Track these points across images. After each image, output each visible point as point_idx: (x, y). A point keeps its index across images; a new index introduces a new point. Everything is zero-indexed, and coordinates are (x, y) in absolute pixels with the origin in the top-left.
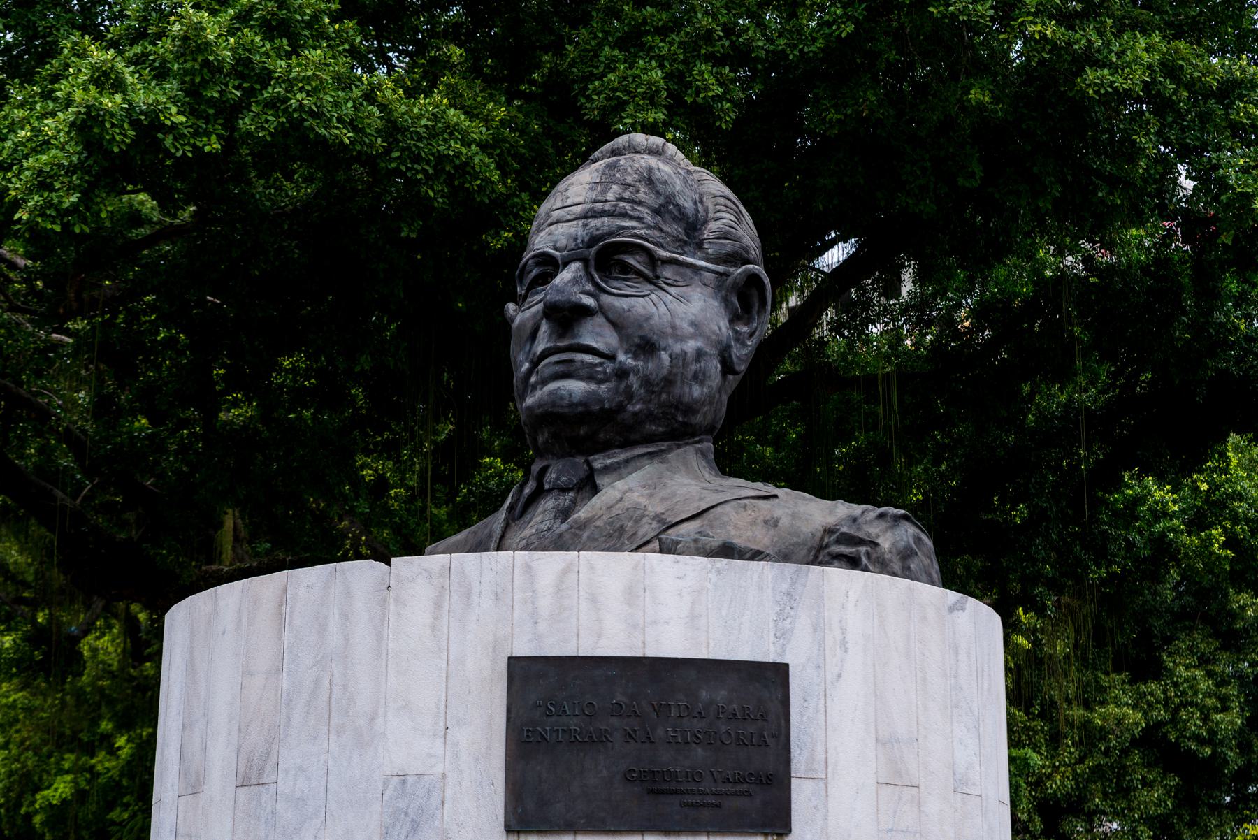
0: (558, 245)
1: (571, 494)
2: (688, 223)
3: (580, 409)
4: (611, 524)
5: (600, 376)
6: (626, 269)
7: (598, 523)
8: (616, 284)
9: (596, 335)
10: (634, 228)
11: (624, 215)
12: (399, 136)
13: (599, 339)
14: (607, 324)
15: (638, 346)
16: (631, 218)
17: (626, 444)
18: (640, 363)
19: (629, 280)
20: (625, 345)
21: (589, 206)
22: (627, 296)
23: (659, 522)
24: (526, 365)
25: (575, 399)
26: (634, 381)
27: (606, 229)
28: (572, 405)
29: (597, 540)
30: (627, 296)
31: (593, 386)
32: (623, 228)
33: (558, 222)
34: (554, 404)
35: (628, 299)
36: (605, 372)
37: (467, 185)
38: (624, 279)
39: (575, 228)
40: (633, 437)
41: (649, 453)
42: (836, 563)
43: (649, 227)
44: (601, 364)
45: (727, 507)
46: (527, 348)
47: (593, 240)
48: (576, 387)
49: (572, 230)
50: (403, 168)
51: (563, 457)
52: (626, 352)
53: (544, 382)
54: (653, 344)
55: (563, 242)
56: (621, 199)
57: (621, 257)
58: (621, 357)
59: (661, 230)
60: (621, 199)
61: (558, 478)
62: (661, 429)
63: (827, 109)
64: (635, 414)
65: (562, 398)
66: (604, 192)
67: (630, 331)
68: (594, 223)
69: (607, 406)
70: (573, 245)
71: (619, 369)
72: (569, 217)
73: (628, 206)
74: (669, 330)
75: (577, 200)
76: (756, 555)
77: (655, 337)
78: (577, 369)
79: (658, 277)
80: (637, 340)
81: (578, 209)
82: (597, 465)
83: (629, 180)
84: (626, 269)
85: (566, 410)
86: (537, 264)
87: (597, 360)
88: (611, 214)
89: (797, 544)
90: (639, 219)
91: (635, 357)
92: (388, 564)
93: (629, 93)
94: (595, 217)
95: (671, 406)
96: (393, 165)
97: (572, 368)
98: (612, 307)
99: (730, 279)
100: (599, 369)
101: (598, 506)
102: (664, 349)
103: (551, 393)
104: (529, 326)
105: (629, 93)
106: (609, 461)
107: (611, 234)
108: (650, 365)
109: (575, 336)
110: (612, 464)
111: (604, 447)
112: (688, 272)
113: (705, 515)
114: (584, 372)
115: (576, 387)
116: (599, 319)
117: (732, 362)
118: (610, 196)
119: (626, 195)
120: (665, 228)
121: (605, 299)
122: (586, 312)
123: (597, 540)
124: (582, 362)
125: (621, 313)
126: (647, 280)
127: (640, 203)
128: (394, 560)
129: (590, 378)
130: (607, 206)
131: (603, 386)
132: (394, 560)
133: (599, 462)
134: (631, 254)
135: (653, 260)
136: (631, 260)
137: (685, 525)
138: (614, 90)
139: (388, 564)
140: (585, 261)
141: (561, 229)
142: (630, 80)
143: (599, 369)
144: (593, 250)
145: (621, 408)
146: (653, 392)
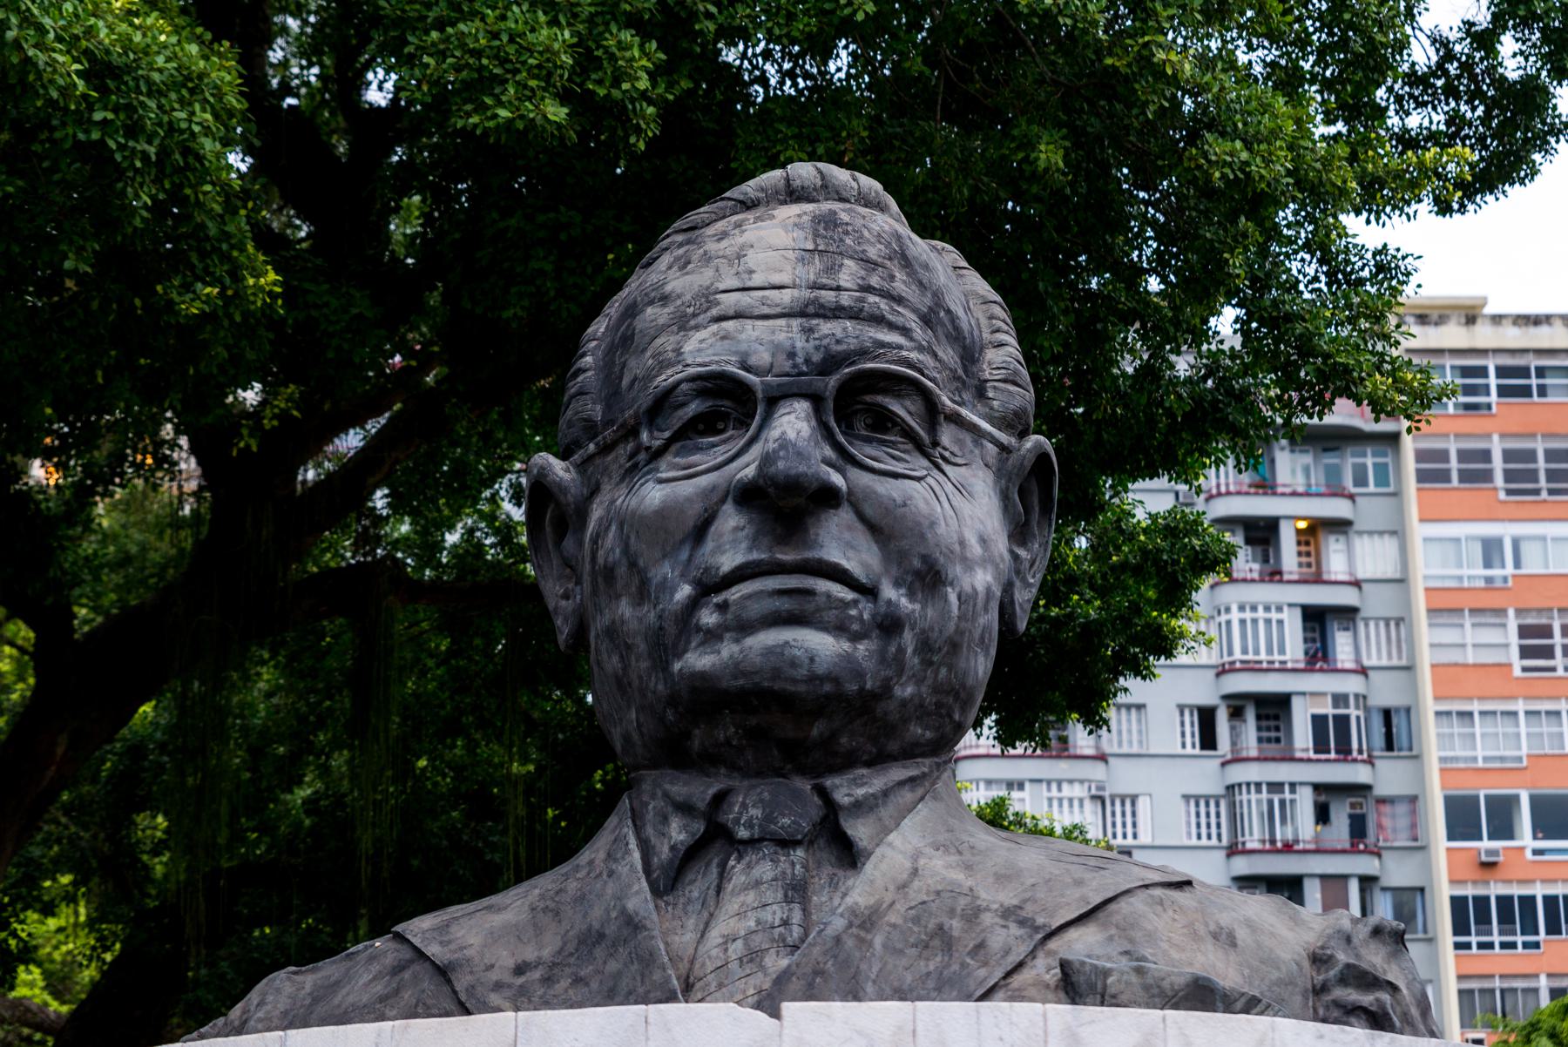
0: (753, 361)
1: (800, 852)
2: (964, 347)
3: (828, 687)
4: (916, 920)
5: (855, 627)
6: (883, 423)
7: (893, 918)
8: (869, 450)
9: (841, 543)
10: (900, 347)
11: (878, 320)
12: (111, 84)
13: (851, 553)
14: (859, 525)
15: (918, 574)
16: (892, 326)
17: (879, 760)
18: (917, 607)
19: (893, 444)
20: (894, 571)
21: (807, 294)
22: (896, 476)
23: (1022, 923)
24: (685, 591)
25: (820, 669)
26: (908, 639)
27: (853, 344)
28: (813, 678)
29: (901, 952)
30: (896, 476)
31: (846, 646)
32: (882, 345)
33: (738, 316)
34: (776, 673)
35: (900, 482)
36: (860, 618)
37: (188, 191)
38: (883, 442)
39: (787, 333)
40: (893, 746)
41: (912, 780)
42: (1353, 1020)
43: (920, 349)
44: (855, 602)
45: (1137, 903)
46: (684, 555)
47: (831, 362)
48: (820, 645)
49: (781, 337)
50: (112, 145)
51: (759, 774)
52: (897, 584)
53: (745, 628)
54: (938, 573)
55: (762, 357)
56: (868, 289)
57: (880, 399)
58: (889, 592)
59: (935, 355)
60: (868, 289)
61: (768, 818)
62: (928, 734)
63: (784, 140)
64: (904, 703)
65: (794, 663)
66: (832, 269)
67: (904, 544)
68: (826, 327)
69: (869, 686)
70: (787, 366)
71: (886, 616)
72: (766, 310)
73: (884, 305)
74: (957, 548)
75: (777, 279)
76: (1251, 1005)
77: (942, 560)
78: (818, 610)
79: (936, 444)
80: (916, 563)
81: (786, 297)
82: (842, 796)
83: (873, 252)
84: (883, 423)
85: (802, 688)
86: (701, 393)
87: (848, 595)
88: (854, 314)
89: (1280, 982)
90: (905, 331)
91: (911, 595)
92: (775, 1014)
93: (503, 62)
94: (824, 317)
95: (948, 693)
96: (95, 135)
97: (810, 607)
98: (870, 494)
99: (1014, 456)
100: (853, 612)
101: (879, 883)
102: (951, 584)
103: (769, 651)
104: (694, 512)
105: (503, 62)
106: (860, 792)
107: (863, 353)
108: (930, 612)
109: (808, 544)
110: (866, 797)
111: (846, 763)
112: (968, 438)
113: (1101, 915)
114: (831, 616)
115: (820, 645)
116: (845, 515)
117: (1014, 613)
118: (845, 279)
119: (875, 281)
120: (940, 354)
121: (863, 479)
122: (828, 497)
123: (901, 952)
124: (828, 595)
125: (892, 509)
126: (921, 449)
127: (899, 300)
128: (788, 1008)
129: (839, 629)
130: (846, 299)
131: (861, 647)
132: (788, 1008)
133: (844, 790)
134: (898, 396)
135: (933, 412)
136: (897, 408)
137: (1073, 934)
138: (477, 53)
139: (775, 1014)
140: (816, 400)
141: (752, 332)
142: (505, 38)
143: (853, 612)
144: (833, 381)
145: (885, 690)
146: (931, 663)
